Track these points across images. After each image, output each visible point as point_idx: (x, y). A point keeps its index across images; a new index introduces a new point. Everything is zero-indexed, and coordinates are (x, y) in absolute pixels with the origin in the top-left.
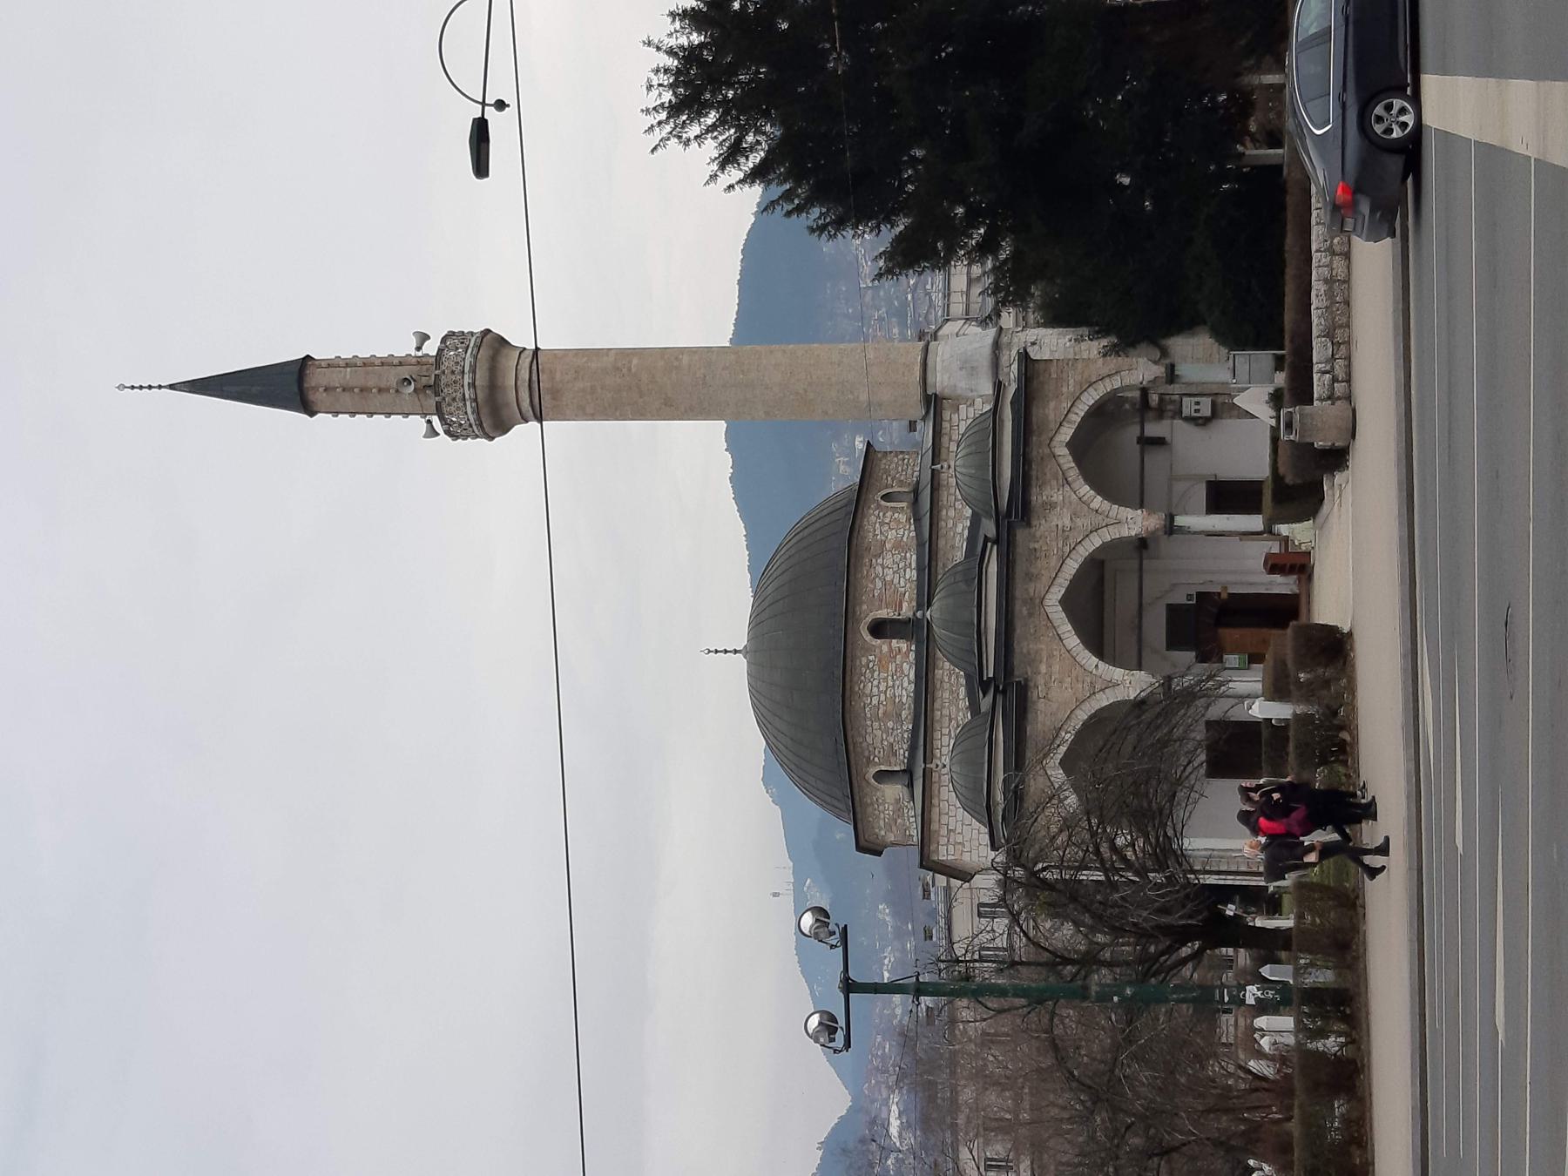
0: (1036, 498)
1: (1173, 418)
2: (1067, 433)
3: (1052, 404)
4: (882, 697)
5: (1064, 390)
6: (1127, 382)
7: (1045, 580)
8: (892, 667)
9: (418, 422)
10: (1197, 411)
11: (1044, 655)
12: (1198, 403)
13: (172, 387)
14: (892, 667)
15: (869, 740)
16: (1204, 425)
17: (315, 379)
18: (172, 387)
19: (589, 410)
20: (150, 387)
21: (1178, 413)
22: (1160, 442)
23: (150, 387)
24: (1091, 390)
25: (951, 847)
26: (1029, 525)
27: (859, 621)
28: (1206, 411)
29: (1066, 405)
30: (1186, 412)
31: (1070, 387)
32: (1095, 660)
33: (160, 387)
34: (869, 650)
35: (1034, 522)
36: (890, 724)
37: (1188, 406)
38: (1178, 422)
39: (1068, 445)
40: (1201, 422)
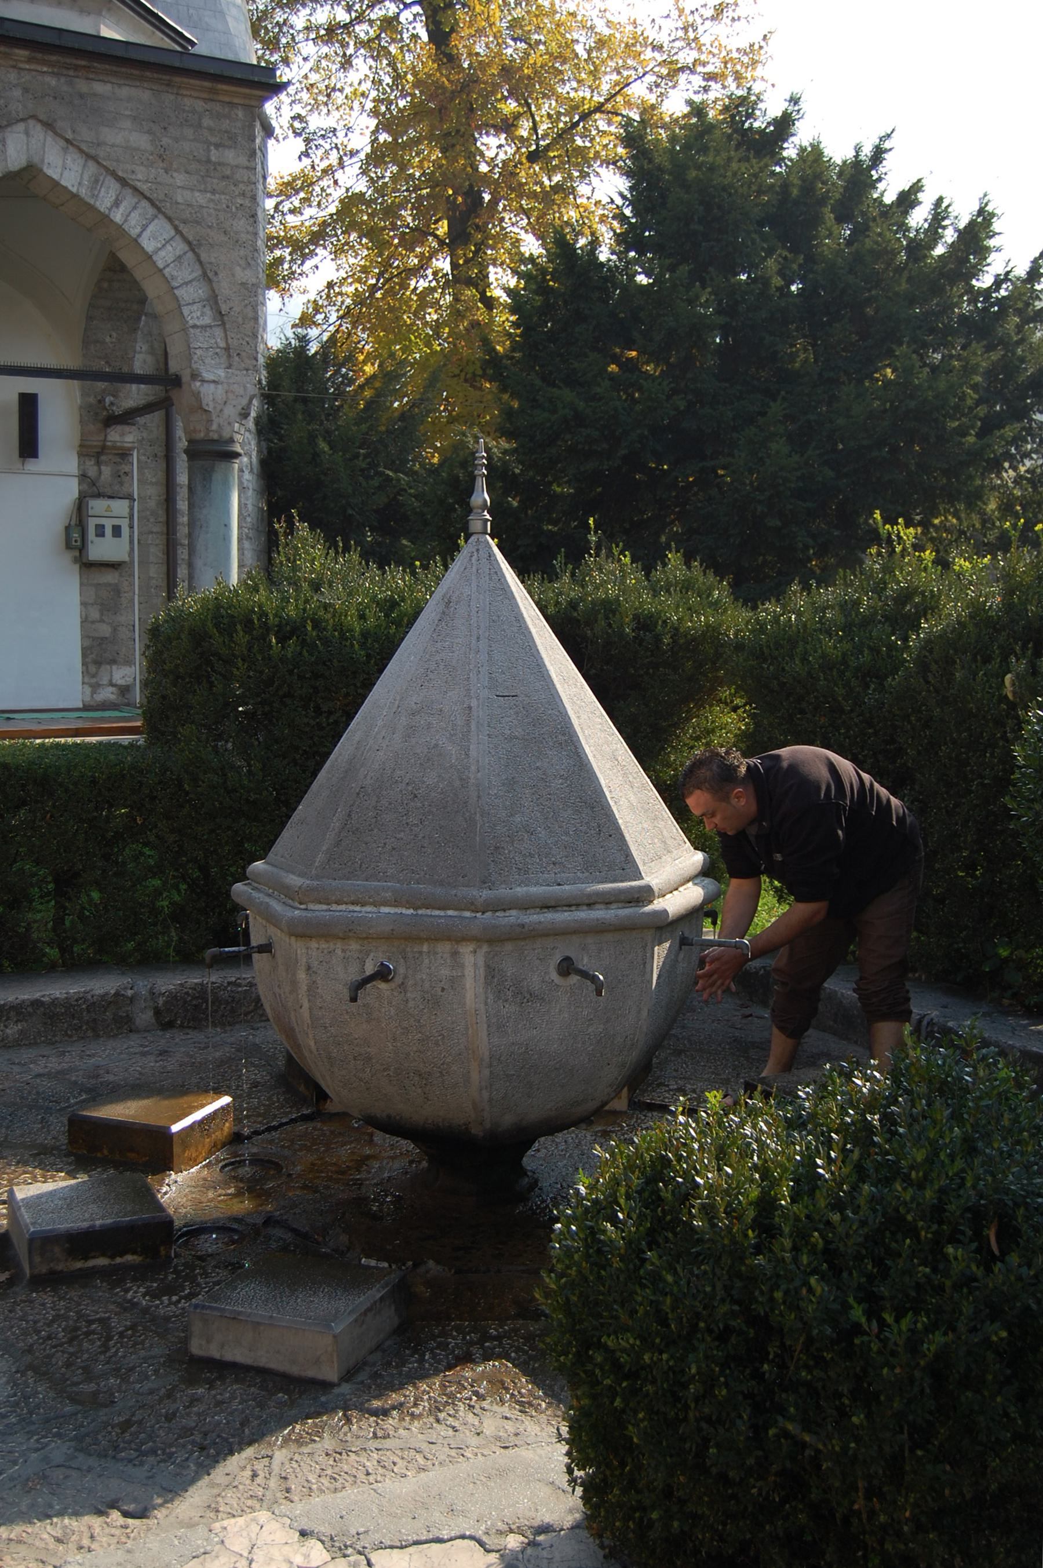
1: (83, 477)
2: (66, 171)
3: (141, 140)
5: (180, 179)
6: (200, 341)
10: (100, 531)
12: (117, 531)
16: (68, 546)
21: (91, 488)
22: (28, 446)
24: (180, 247)
28: (101, 549)
29: (140, 176)
30: (97, 506)
31: (185, 190)
37: (110, 511)
38: (72, 489)
39: (31, 172)
40: (76, 536)
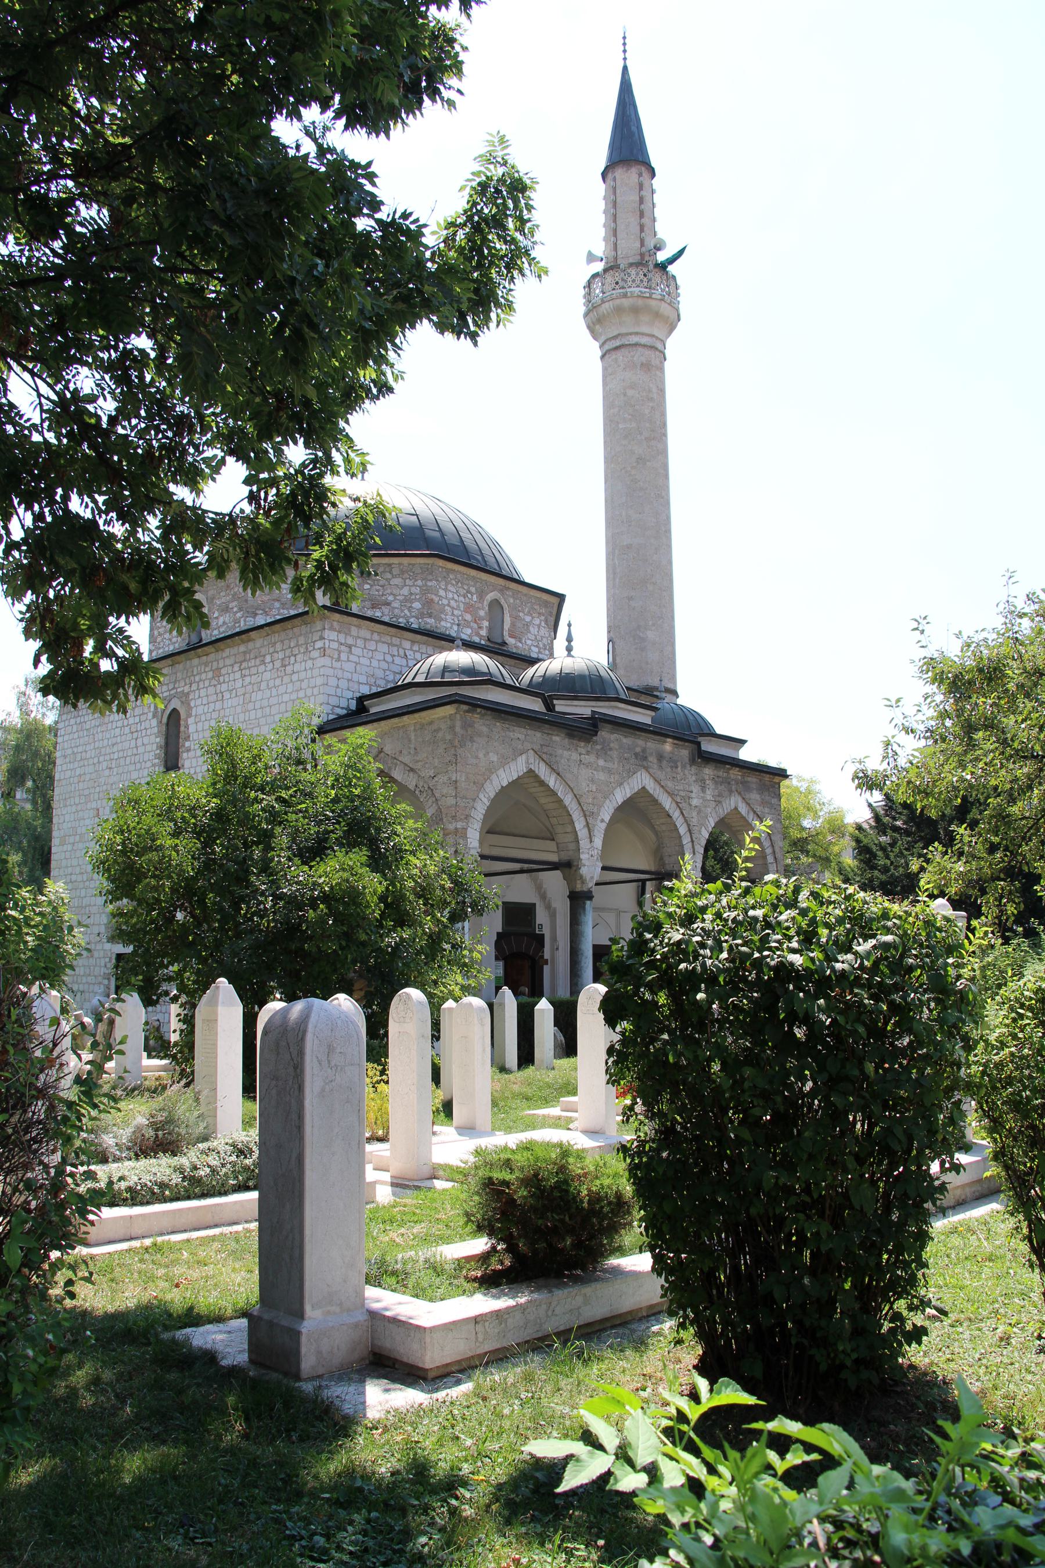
0: (708, 771)
3: (758, 797)
4: (445, 602)
7: (660, 775)
8: (468, 617)
9: (599, 248)
11: (610, 765)
13: (625, 69)
14: (468, 617)
15: (397, 581)
17: (628, 176)
18: (625, 69)
19: (630, 393)
20: (625, 51)
23: (625, 51)
25: (335, 645)
26: (693, 762)
27: (502, 591)
32: (607, 818)
33: (625, 59)
34: (481, 596)
35: (694, 768)
36: (417, 605)
